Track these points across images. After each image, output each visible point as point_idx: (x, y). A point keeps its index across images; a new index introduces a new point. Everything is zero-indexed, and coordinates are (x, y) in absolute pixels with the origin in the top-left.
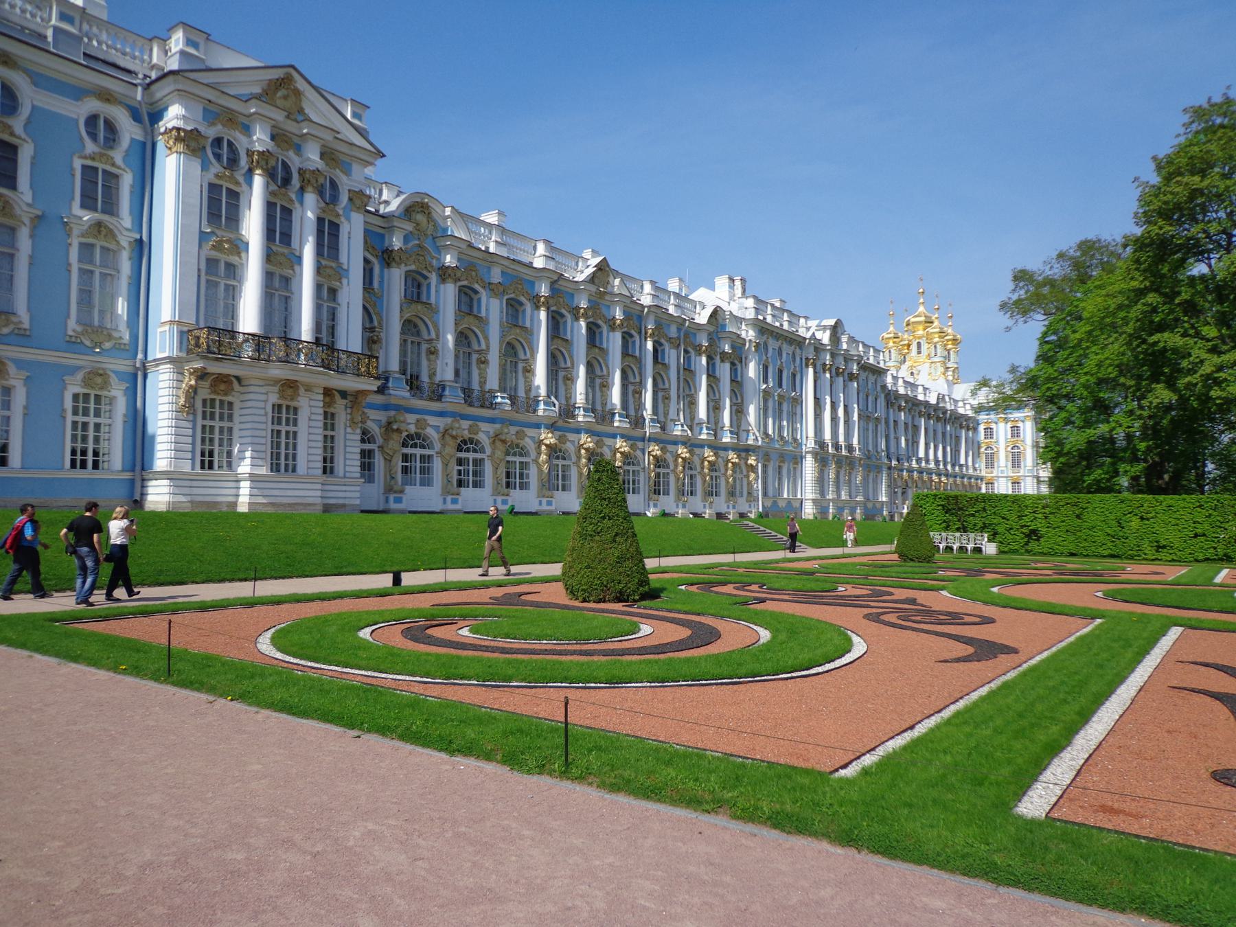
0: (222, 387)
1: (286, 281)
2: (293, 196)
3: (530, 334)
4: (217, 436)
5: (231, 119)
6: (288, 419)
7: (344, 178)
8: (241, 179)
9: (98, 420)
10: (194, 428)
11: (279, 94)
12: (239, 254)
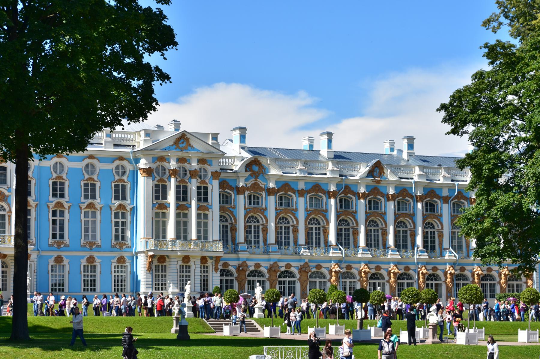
0: (162, 260)
1: (185, 215)
2: (187, 181)
3: (325, 213)
4: (160, 278)
5: (162, 159)
6: (186, 271)
7: (209, 167)
8: (166, 180)
9: (122, 274)
10: (152, 276)
11: (181, 142)
12: (166, 209)
